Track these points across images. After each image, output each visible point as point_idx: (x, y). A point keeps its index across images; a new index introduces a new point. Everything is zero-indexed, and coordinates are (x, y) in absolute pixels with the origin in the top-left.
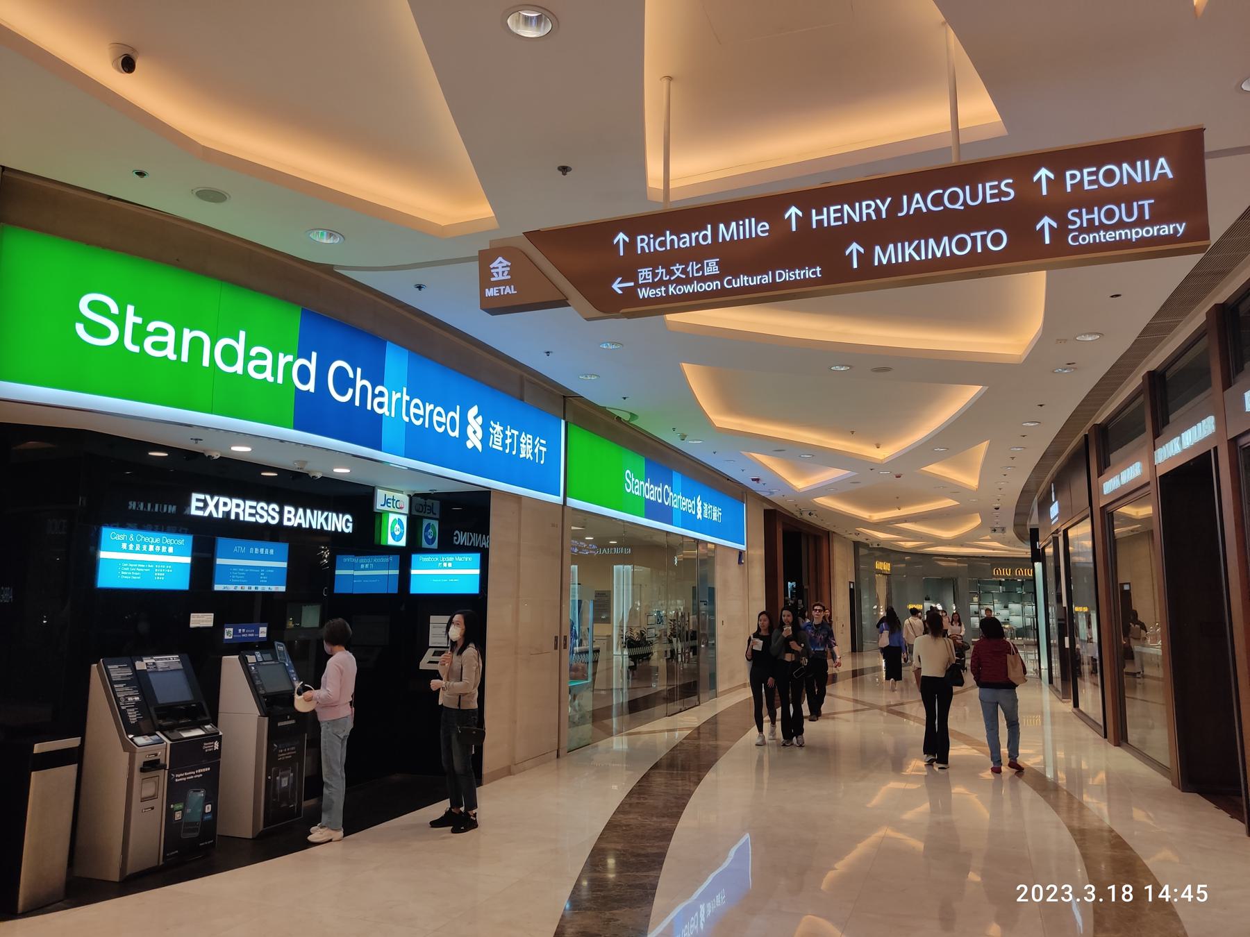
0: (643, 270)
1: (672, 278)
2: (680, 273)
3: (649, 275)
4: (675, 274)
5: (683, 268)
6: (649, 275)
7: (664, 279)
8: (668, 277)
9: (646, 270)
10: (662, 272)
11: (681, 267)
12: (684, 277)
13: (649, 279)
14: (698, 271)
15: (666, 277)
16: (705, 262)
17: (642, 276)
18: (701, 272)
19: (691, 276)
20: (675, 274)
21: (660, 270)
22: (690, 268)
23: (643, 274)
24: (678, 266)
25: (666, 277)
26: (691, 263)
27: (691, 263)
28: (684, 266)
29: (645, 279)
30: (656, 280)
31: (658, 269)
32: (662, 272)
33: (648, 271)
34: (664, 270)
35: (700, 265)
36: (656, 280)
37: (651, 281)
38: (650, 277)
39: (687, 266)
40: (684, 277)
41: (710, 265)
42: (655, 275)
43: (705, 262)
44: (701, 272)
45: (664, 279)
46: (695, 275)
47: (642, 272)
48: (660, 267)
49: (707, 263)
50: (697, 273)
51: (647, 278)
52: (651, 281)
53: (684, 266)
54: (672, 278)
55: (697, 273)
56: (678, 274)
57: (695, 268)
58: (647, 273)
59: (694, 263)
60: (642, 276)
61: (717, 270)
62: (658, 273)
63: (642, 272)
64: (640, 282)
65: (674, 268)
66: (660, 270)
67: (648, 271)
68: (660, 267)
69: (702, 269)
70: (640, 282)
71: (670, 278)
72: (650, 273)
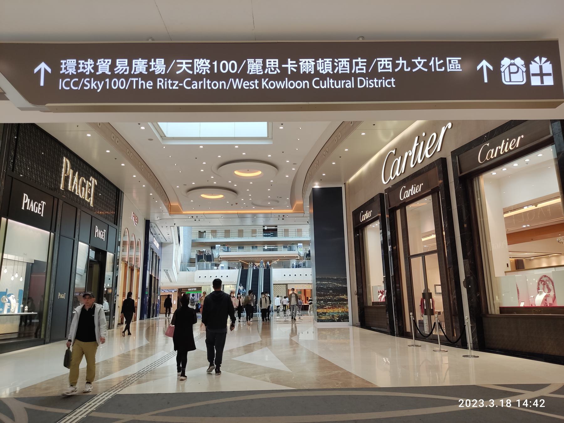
0: (383, 59)
1: (414, 70)
2: (422, 66)
3: (388, 65)
4: (417, 66)
5: (424, 62)
6: (388, 65)
7: (405, 70)
8: (409, 69)
9: (386, 59)
10: (403, 64)
11: (423, 61)
12: (426, 70)
13: (389, 69)
14: (440, 66)
15: (407, 68)
16: (448, 59)
17: (381, 65)
18: (443, 68)
19: (433, 70)
20: (417, 66)
21: (401, 61)
22: (432, 63)
23: (383, 63)
24: (419, 59)
25: (407, 68)
26: (433, 58)
27: (433, 58)
28: (426, 60)
29: (384, 68)
30: (396, 70)
31: (399, 60)
32: (403, 64)
33: (388, 61)
34: (405, 62)
35: (442, 61)
36: (396, 70)
37: (391, 71)
38: (390, 66)
39: (429, 61)
40: (426, 70)
41: (452, 63)
42: (395, 66)
43: (448, 59)
44: (443, 68)
45: (405, 70)
46: (438, 70)
47: (381, 61)
48: (401, 58)
49: (450, 61)
50: (439, 68)
51: (387, 67)
52: (391, 71)
53: (426, 60)
54: (414, 70)
55: (439, 68)
56: (420, 67)
57: (437, 63)
58: (386, 63)
59: (437, 58)
60: (381, 65)
61: (459, 67)
62: (399, 64)
63: (381, 61)
64: (380, 71)
65: (416, 61)
66: (401, 61)
67: (388, 61)
68: (401, 58)
69: (444, 65)
70: (380, 71)
71: (411, 70)
72: (390, 63)
